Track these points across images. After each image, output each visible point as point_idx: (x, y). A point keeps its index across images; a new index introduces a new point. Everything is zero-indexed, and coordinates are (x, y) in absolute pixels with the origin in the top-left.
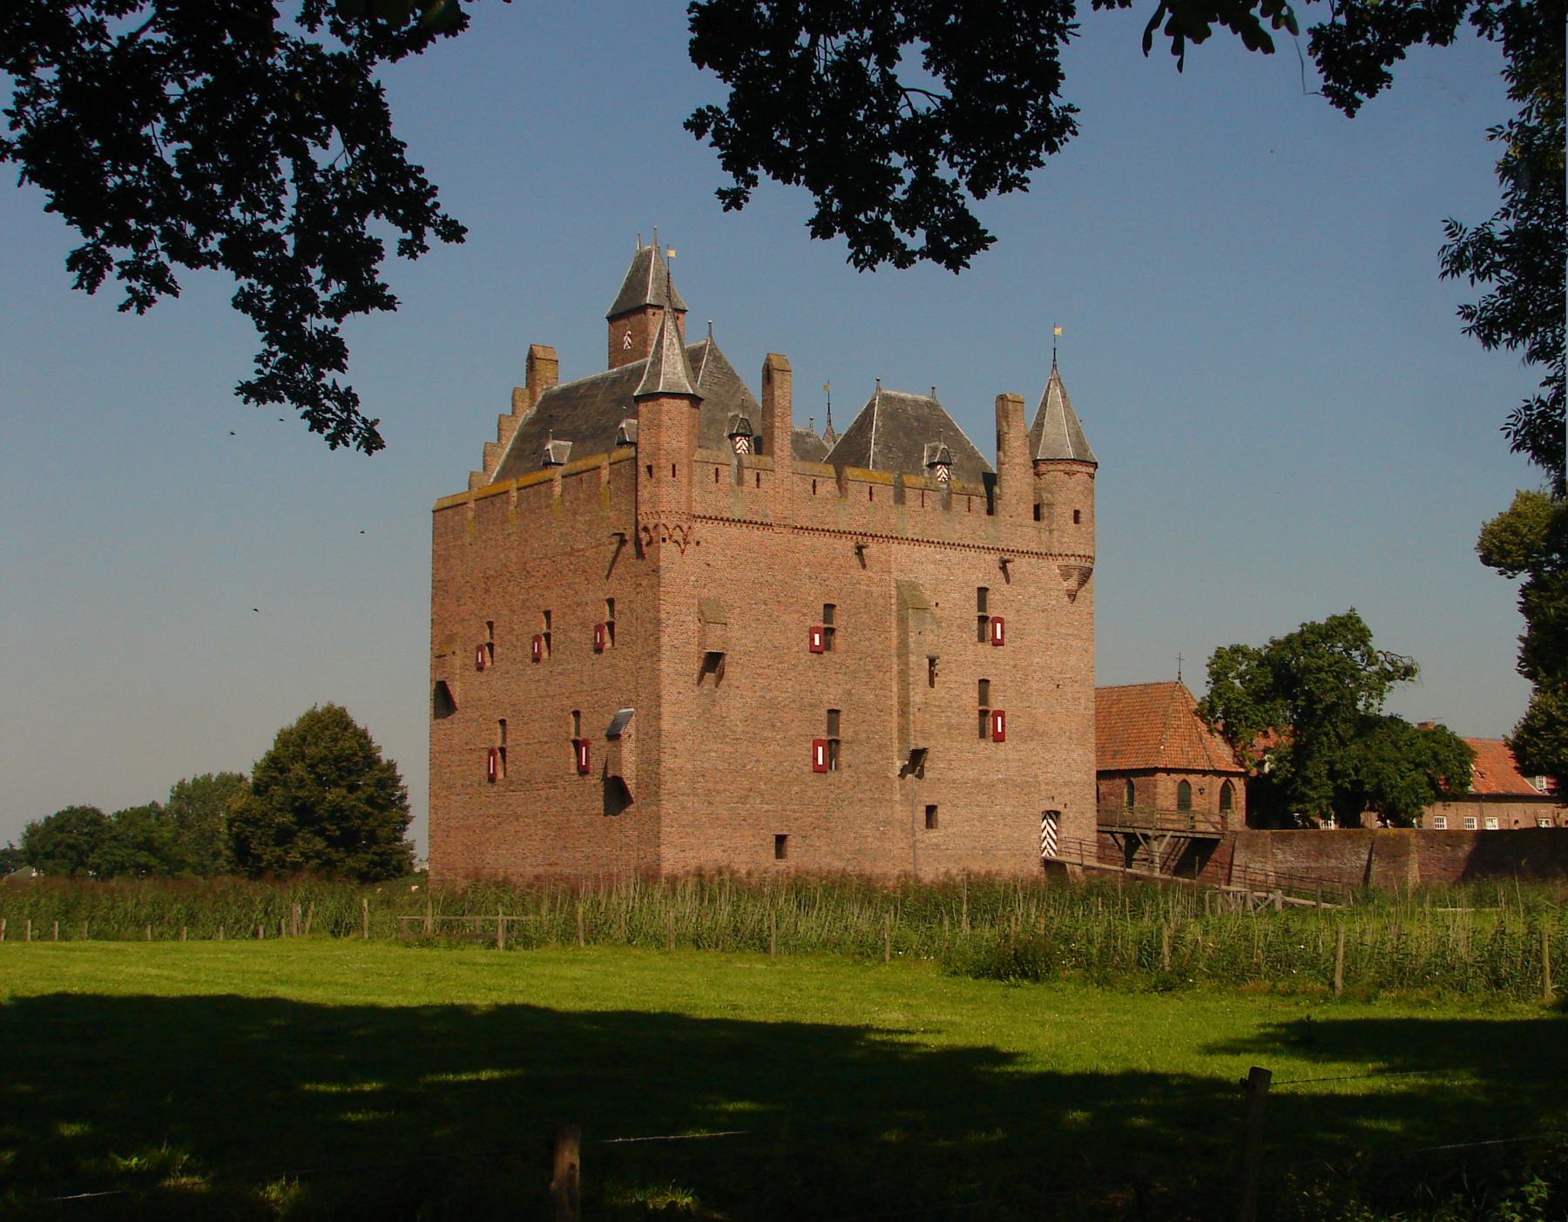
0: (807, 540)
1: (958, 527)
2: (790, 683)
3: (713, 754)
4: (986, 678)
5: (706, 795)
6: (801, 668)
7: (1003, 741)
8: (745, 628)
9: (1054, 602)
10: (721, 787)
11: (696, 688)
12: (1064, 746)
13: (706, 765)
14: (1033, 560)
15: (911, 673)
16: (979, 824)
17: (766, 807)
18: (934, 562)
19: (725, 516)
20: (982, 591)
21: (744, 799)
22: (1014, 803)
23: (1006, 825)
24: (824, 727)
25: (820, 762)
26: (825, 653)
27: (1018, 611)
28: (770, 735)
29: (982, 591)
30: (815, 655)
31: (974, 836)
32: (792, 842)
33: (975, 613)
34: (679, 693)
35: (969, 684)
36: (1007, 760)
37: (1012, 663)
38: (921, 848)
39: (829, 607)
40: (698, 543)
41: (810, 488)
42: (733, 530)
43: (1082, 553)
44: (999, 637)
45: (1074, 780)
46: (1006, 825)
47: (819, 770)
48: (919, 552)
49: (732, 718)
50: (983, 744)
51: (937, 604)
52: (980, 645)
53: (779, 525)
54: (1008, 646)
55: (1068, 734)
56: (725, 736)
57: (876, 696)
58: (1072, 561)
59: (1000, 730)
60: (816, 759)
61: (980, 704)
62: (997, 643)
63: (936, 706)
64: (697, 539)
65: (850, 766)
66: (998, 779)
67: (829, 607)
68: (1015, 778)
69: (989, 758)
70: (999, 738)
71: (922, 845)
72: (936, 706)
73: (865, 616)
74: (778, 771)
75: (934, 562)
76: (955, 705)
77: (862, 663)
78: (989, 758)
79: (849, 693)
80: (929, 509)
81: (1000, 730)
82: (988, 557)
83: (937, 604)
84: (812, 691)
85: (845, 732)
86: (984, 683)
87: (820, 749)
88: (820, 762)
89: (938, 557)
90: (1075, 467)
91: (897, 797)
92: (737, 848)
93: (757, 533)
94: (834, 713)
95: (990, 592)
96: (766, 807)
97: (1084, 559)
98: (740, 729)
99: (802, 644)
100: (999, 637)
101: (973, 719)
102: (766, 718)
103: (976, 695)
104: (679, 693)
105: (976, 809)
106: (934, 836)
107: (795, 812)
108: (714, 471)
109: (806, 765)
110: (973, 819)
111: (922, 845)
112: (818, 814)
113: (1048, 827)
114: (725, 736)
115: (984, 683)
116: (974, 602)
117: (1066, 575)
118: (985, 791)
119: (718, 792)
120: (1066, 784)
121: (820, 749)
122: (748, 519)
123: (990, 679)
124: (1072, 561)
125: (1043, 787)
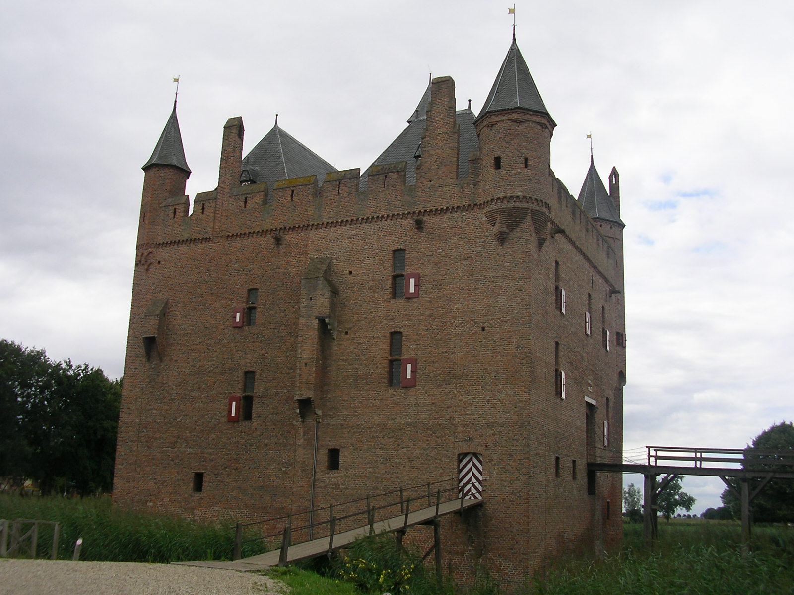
0: (238, 243)
1: (373, 203)
2: (216, 354)
3: (154, 411)
4: (398, 330)
5: (147, 441)
6: (225, 341)
7: (414, 386)
8: (186, 317)
9: (480, 249)
10: (157, 435)
11: (147, 364)
12: (489, 388)
13: (149, 420)
14: (456, 215)
15: (300, 333)
16: (382, 466)
17: (189, 450)
19: (177, 239)
21: (173, 445)
22: (424, 445)
23: (413, 467)
24: (240, 386)
25: (233, 414)
26: (246, 328)
27: (436, 264)
28: (197, 395)
30: (237, 330)
31: (377, 477)
32: (206, 479)
33: (387, 272)
34: (136, 369)
35: (378, 337)
36: (417, 405)
37: (428, 313)
38: (320, 487)
40: (159, 262)
41: (242, 204)
43: (501, 195)
44: (412, 290)
45: (500, 421)
46: (413, 467)
47: (232, 420)
48: (334, 232)
49: (170, 384)
50: (391, 391)
51: (350, 273)
52: (392, 301)
53: (217, 237)
55: (493, 375)
56: (164, 397)
57: (287, 356)
58: (493, 206)
59: (409, 376)
60: (230, 412)
61: (391, 355)
63: (343, 360)
64: (158, 260)
65: (259, 416)
66: (408, 424)
68: (425, 422)
69: (397, 404)
70: (410, 385)
71: (322, 484)
72: (343, 360)
73: (282, 293)
74: (200, 423)
76: (363, 358)
77: (276, 331)
78: (397, 404)
79: (264, 357)
80: (345, 195)
81: (409, 376)
82: (404, 222)
83: (350, 273)
84: (232, 359)
85: (259, 389)
86: (396, 337)
87: (234, 403)
88: (233, 414)
89: (354, 232)
91: (301, 442)
92: (165, 481)
94: (249, 375)
95: (407, 252)
96: (189, 450)
97: (505, 202)
98: (175, 392)
99: (227, 323)
100: (412, 290)
101: (382, 369)
102: (195, 382)
103: (386, 346)
104: (136, 369)
105: (380, 452)
106: (334, 477)
107: (211, 454)
108: (173, 211)
109: (222, 417)
110: (376, 461)
111: (322, 484)
112: (230, 456)
113: (474, 469)
114: (164, 397)
115: (396, 337)
117: (492, 221)
118: (391, 435)
119: (156, 439)
120: (489, 425)
121: (234, 403)
122: (193, 238)
123: (402, 330)
124: (493, 206)
125: (459, 429)
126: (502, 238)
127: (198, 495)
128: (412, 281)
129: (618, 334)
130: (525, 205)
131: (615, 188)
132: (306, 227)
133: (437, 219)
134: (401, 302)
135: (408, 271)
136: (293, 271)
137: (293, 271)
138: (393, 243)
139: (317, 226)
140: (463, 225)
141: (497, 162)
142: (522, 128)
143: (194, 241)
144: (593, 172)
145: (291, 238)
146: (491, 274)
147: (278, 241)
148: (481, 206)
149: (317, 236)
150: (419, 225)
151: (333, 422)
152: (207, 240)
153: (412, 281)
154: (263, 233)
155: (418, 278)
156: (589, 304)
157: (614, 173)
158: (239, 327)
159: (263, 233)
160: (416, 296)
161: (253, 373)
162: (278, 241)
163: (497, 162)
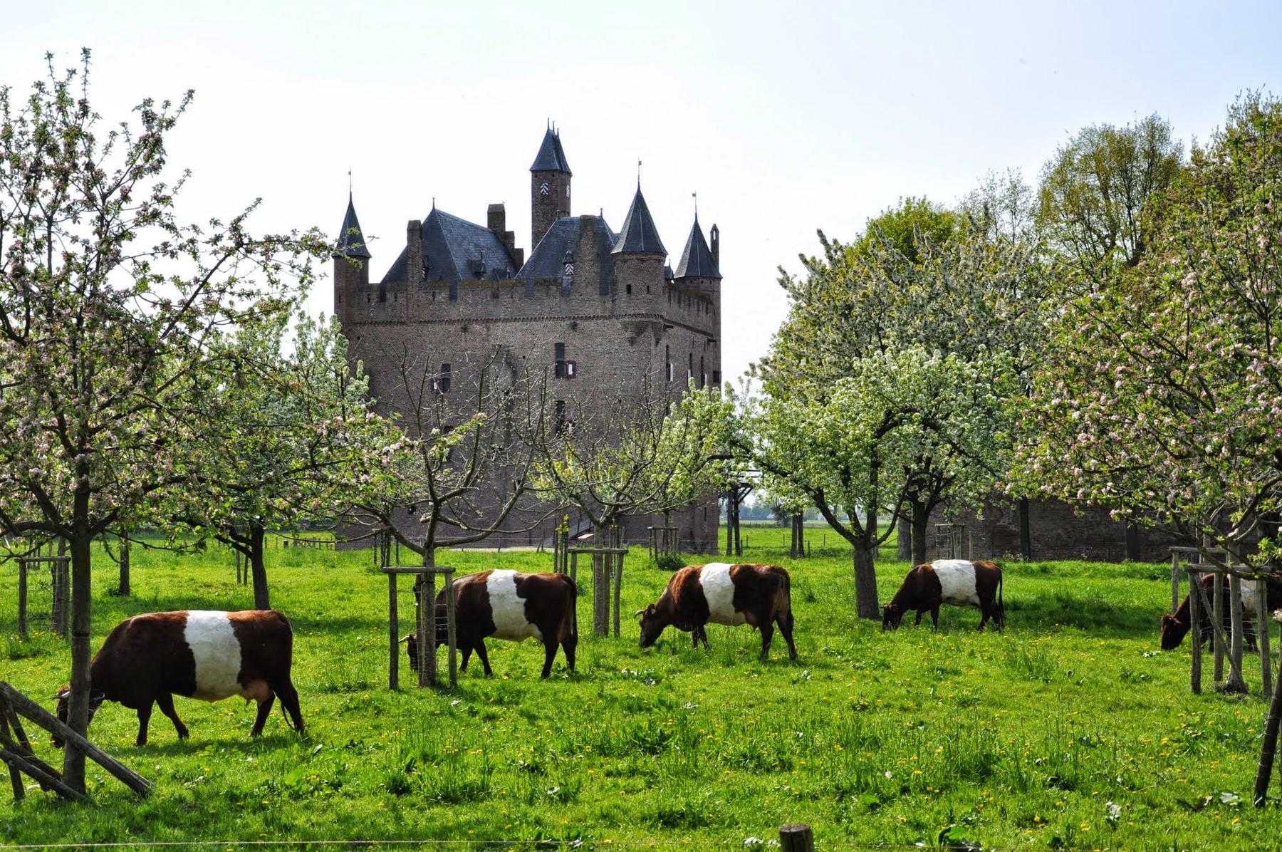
14: (600, 321)
18: (522, 331)
20: (560, 348)
29: (560, 348)
39: (446, 367)
41: (431, 297)
42: (381, 328)
44: (571, 372)
48: (510, 326)
54: (580, 378)
58: (627, 320)
62: (569, 377)
67: (446, 367)
75: (522, 331)
82: (563, 323)
90: (626, 257)
93: (396, 328)
100: (571, 372)
116: (552, 353)
117: (625, 327)
124: (627, 320)
126: (632, 341)
128: (570, 367)
129: (714, 372)
130: (647, 320)
131: (715, 244)
132: (487, 321)
133: (586, 323)
135: (567, 358)
138: (554, 338)
140: (606, 329)
141: (629, 288)
142: (645, 264)
144: (697, 230)
146: (624, 365)
147: (465, 329)
148: (617, 317)
150: (574, 327)
153: (570, 367)
154: (451, 322)
155: (574, 363)
156: (691, 363)
157: (715, 229)
160: (574, 376)
163: (629, 288)
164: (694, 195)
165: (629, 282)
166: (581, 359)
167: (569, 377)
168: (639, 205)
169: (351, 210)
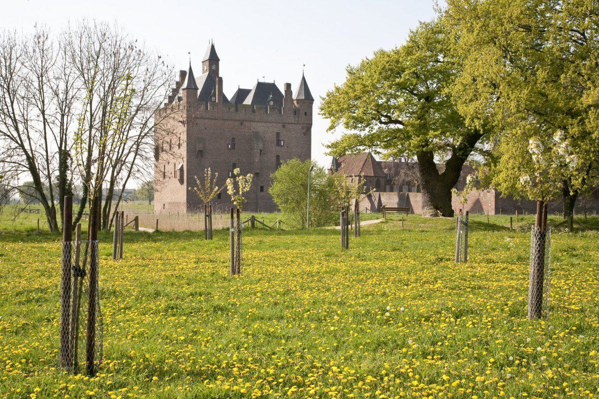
1: (271, 118)
20: (278, 134)
29: (278, 134)
33: (274, 138)
39: (233, 139)
41: (228, 110)
42: (206, 121)
48: (259, 124)
58: (304, 125)
67: (233, 139)
93: (213, 121)
106: (262, 194)
116: (275, 136)
124: (304, 125)
127: (220, 200)
132: (250, 121)
134: (279, 148)
136: (247, 134)
137: (247, 134)
138: (276, 130)
139: (254, 122)
143: (211, 119)
145: (246, 123)
147: (242, 124)
149: (254, 124)
151: (261, 179)
152: (216, 119)
154: (236, 120)
158: (230, 149)
159: (236, 120)
160: (283, 146)
161: (236, 164)
162: (242, 124)
164: (264, 77)
165: (306, 111)
166: (286, 139)
167: (281, 146)
168: (304, 83)
169: (304, 78)
